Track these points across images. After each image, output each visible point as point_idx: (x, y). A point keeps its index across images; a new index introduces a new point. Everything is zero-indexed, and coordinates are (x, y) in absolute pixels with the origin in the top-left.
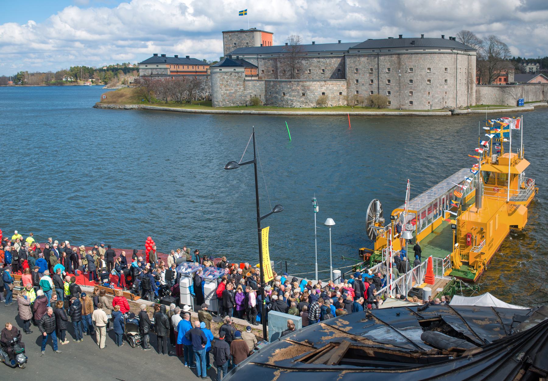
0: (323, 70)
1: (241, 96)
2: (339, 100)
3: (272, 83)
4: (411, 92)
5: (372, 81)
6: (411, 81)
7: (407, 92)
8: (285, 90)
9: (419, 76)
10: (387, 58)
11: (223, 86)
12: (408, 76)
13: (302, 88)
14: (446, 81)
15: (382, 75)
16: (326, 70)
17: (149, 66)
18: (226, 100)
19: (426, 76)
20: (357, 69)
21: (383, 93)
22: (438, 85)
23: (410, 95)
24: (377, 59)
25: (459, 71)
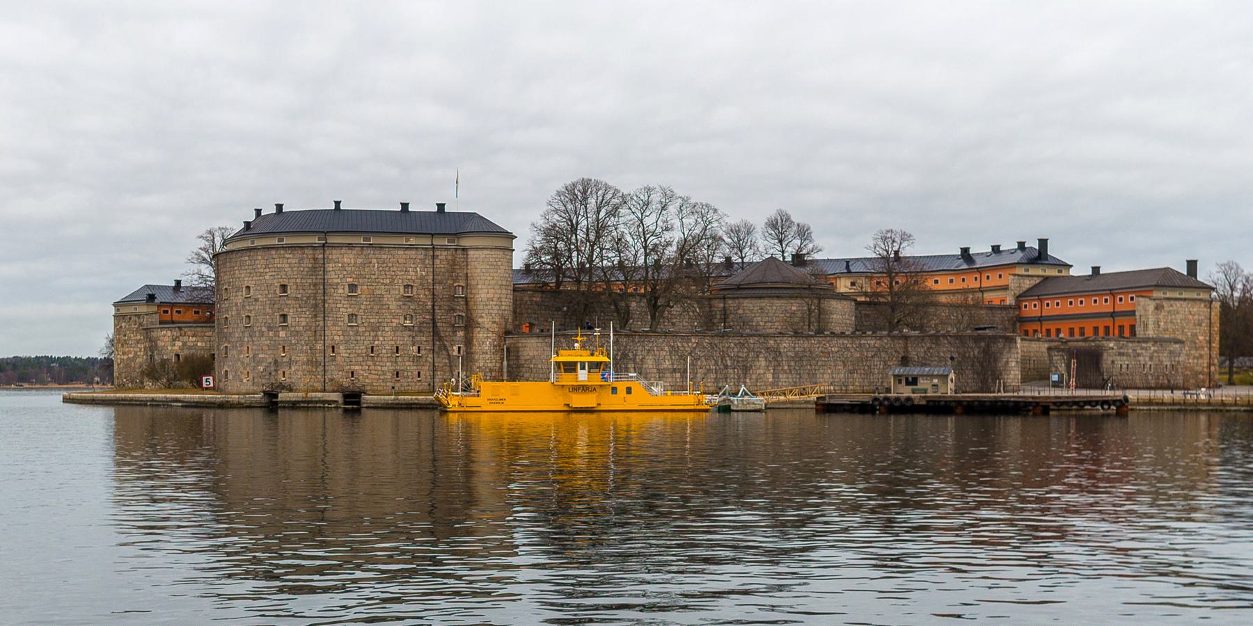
19: (244, 306)
22: (264, 329)
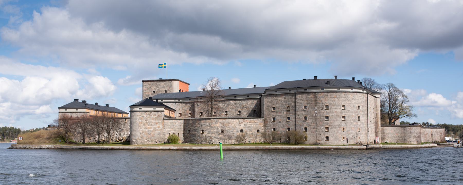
0: (239, 112)
1: (159, 134)
2: (256, 137)
3: (191, 122)
4: (327, 128)
5: (289, 118)
6: (327, 118)
7: (323, 128)
8: (204, 128)
9: (335, 113)
10: (304, 96)
11: (142, 125)
12: (325, 113)
13: (221, 125)
14: (359, 117)
15: (298, 113)
16: (242, 112)
17: (69, 110)
18: (145, 138)
19: (341, 113)
20: (274, 108)
21: (300, 129)
22: (352, 121)
23: (326, 130)
24: (294, 98)
25: (369, 109)
